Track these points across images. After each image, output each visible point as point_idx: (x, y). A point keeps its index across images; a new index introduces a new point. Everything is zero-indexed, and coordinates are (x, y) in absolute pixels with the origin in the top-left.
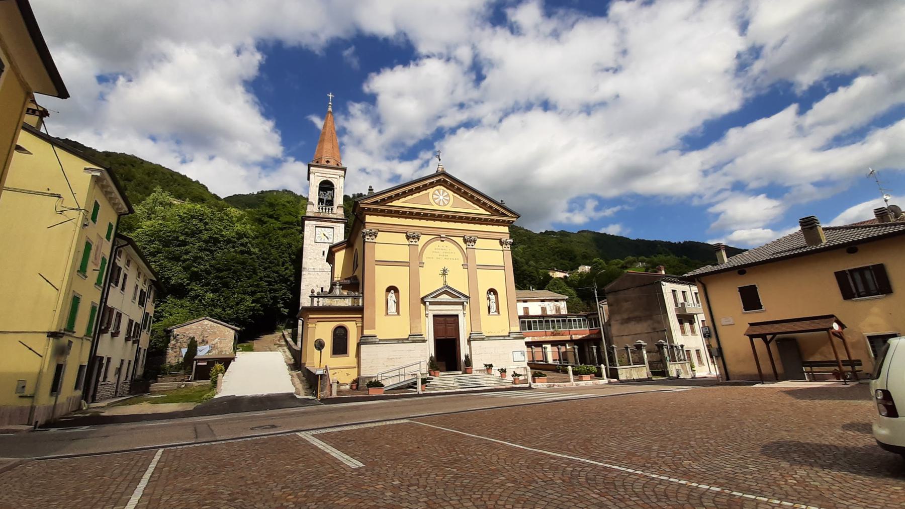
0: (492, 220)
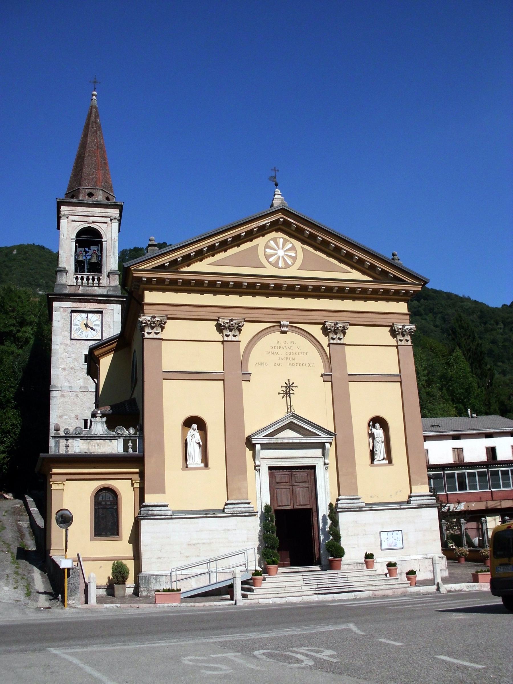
0: (375, 291)
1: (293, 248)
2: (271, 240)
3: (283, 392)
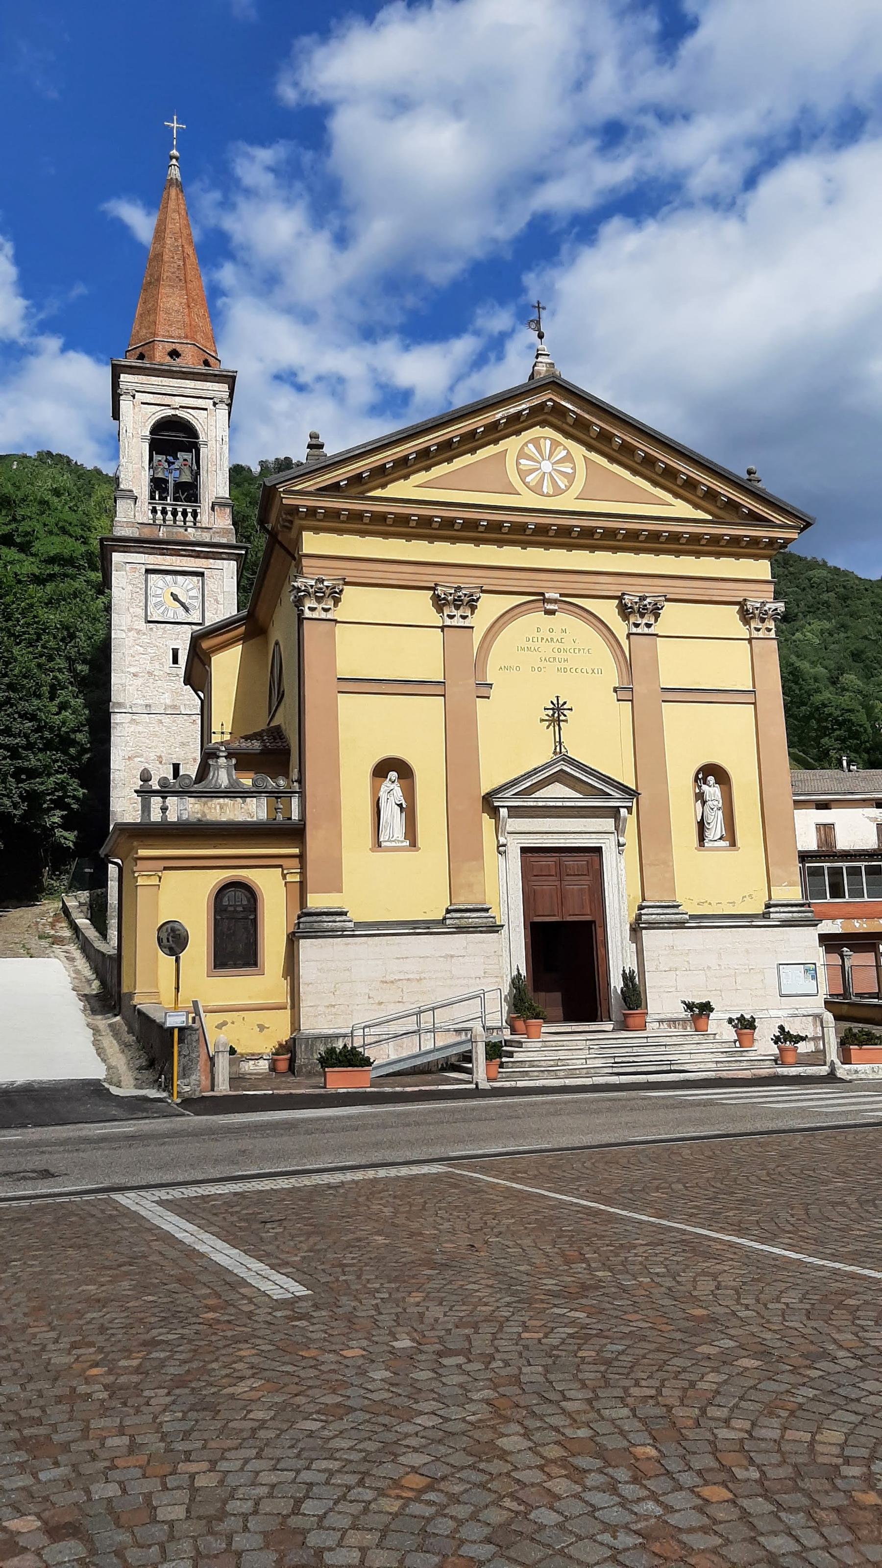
0: (715, 540)
1: (569, 458)
2: (529, 442)
3: (547, 718)
